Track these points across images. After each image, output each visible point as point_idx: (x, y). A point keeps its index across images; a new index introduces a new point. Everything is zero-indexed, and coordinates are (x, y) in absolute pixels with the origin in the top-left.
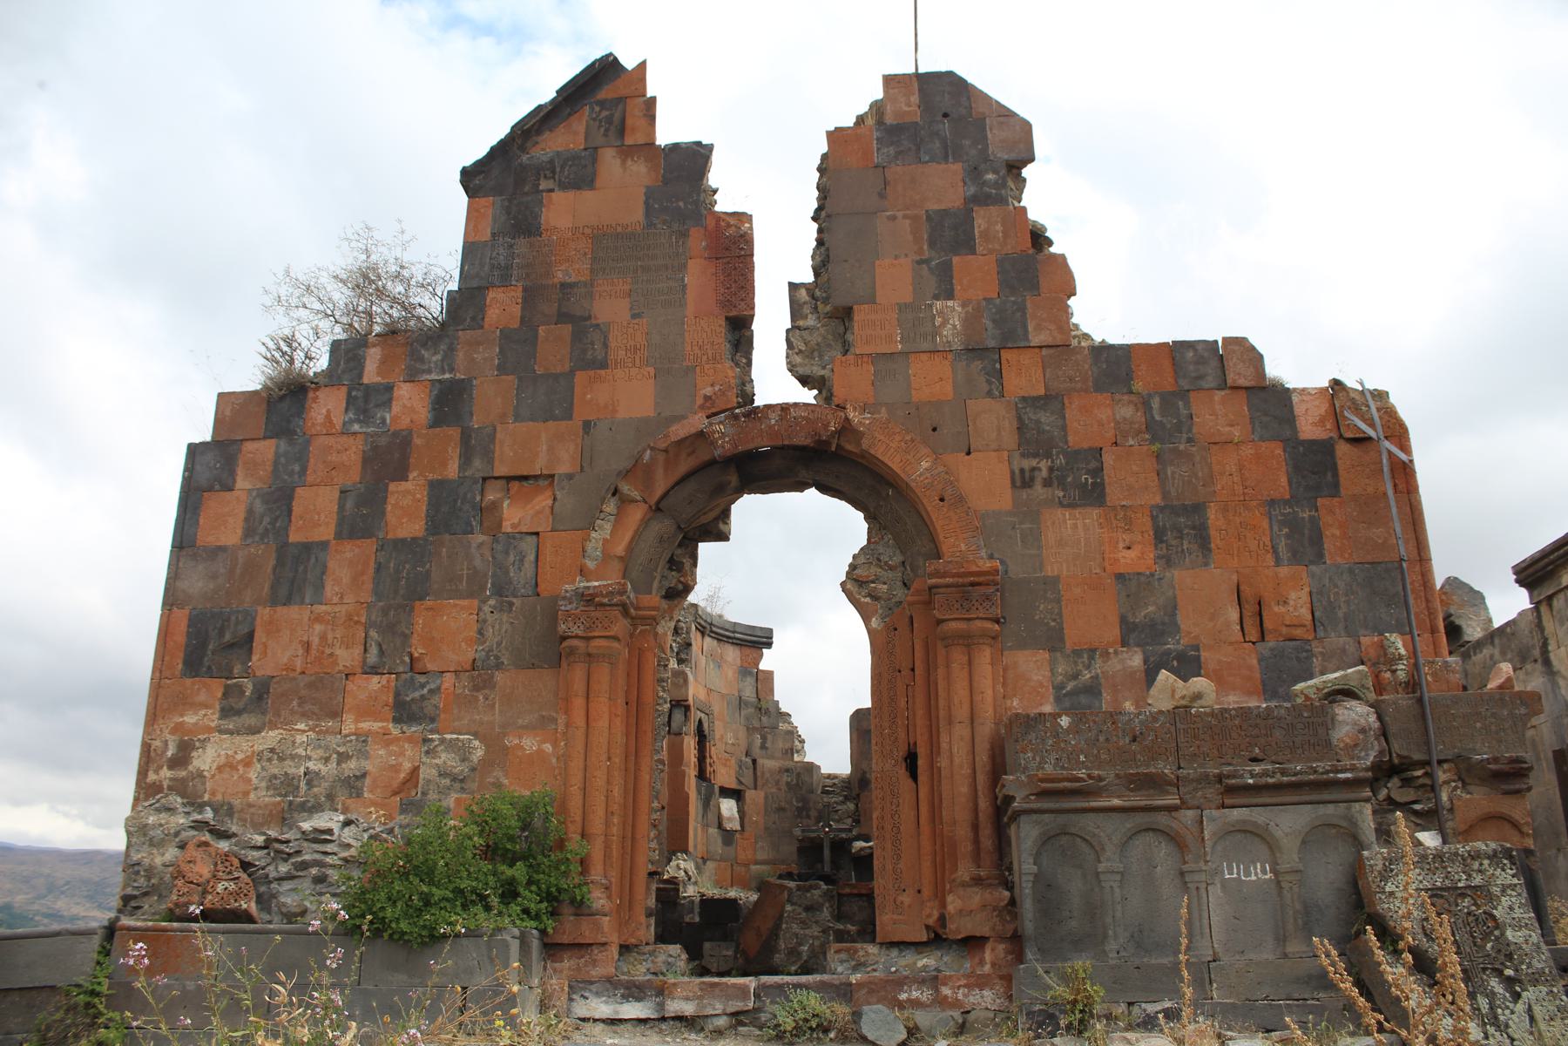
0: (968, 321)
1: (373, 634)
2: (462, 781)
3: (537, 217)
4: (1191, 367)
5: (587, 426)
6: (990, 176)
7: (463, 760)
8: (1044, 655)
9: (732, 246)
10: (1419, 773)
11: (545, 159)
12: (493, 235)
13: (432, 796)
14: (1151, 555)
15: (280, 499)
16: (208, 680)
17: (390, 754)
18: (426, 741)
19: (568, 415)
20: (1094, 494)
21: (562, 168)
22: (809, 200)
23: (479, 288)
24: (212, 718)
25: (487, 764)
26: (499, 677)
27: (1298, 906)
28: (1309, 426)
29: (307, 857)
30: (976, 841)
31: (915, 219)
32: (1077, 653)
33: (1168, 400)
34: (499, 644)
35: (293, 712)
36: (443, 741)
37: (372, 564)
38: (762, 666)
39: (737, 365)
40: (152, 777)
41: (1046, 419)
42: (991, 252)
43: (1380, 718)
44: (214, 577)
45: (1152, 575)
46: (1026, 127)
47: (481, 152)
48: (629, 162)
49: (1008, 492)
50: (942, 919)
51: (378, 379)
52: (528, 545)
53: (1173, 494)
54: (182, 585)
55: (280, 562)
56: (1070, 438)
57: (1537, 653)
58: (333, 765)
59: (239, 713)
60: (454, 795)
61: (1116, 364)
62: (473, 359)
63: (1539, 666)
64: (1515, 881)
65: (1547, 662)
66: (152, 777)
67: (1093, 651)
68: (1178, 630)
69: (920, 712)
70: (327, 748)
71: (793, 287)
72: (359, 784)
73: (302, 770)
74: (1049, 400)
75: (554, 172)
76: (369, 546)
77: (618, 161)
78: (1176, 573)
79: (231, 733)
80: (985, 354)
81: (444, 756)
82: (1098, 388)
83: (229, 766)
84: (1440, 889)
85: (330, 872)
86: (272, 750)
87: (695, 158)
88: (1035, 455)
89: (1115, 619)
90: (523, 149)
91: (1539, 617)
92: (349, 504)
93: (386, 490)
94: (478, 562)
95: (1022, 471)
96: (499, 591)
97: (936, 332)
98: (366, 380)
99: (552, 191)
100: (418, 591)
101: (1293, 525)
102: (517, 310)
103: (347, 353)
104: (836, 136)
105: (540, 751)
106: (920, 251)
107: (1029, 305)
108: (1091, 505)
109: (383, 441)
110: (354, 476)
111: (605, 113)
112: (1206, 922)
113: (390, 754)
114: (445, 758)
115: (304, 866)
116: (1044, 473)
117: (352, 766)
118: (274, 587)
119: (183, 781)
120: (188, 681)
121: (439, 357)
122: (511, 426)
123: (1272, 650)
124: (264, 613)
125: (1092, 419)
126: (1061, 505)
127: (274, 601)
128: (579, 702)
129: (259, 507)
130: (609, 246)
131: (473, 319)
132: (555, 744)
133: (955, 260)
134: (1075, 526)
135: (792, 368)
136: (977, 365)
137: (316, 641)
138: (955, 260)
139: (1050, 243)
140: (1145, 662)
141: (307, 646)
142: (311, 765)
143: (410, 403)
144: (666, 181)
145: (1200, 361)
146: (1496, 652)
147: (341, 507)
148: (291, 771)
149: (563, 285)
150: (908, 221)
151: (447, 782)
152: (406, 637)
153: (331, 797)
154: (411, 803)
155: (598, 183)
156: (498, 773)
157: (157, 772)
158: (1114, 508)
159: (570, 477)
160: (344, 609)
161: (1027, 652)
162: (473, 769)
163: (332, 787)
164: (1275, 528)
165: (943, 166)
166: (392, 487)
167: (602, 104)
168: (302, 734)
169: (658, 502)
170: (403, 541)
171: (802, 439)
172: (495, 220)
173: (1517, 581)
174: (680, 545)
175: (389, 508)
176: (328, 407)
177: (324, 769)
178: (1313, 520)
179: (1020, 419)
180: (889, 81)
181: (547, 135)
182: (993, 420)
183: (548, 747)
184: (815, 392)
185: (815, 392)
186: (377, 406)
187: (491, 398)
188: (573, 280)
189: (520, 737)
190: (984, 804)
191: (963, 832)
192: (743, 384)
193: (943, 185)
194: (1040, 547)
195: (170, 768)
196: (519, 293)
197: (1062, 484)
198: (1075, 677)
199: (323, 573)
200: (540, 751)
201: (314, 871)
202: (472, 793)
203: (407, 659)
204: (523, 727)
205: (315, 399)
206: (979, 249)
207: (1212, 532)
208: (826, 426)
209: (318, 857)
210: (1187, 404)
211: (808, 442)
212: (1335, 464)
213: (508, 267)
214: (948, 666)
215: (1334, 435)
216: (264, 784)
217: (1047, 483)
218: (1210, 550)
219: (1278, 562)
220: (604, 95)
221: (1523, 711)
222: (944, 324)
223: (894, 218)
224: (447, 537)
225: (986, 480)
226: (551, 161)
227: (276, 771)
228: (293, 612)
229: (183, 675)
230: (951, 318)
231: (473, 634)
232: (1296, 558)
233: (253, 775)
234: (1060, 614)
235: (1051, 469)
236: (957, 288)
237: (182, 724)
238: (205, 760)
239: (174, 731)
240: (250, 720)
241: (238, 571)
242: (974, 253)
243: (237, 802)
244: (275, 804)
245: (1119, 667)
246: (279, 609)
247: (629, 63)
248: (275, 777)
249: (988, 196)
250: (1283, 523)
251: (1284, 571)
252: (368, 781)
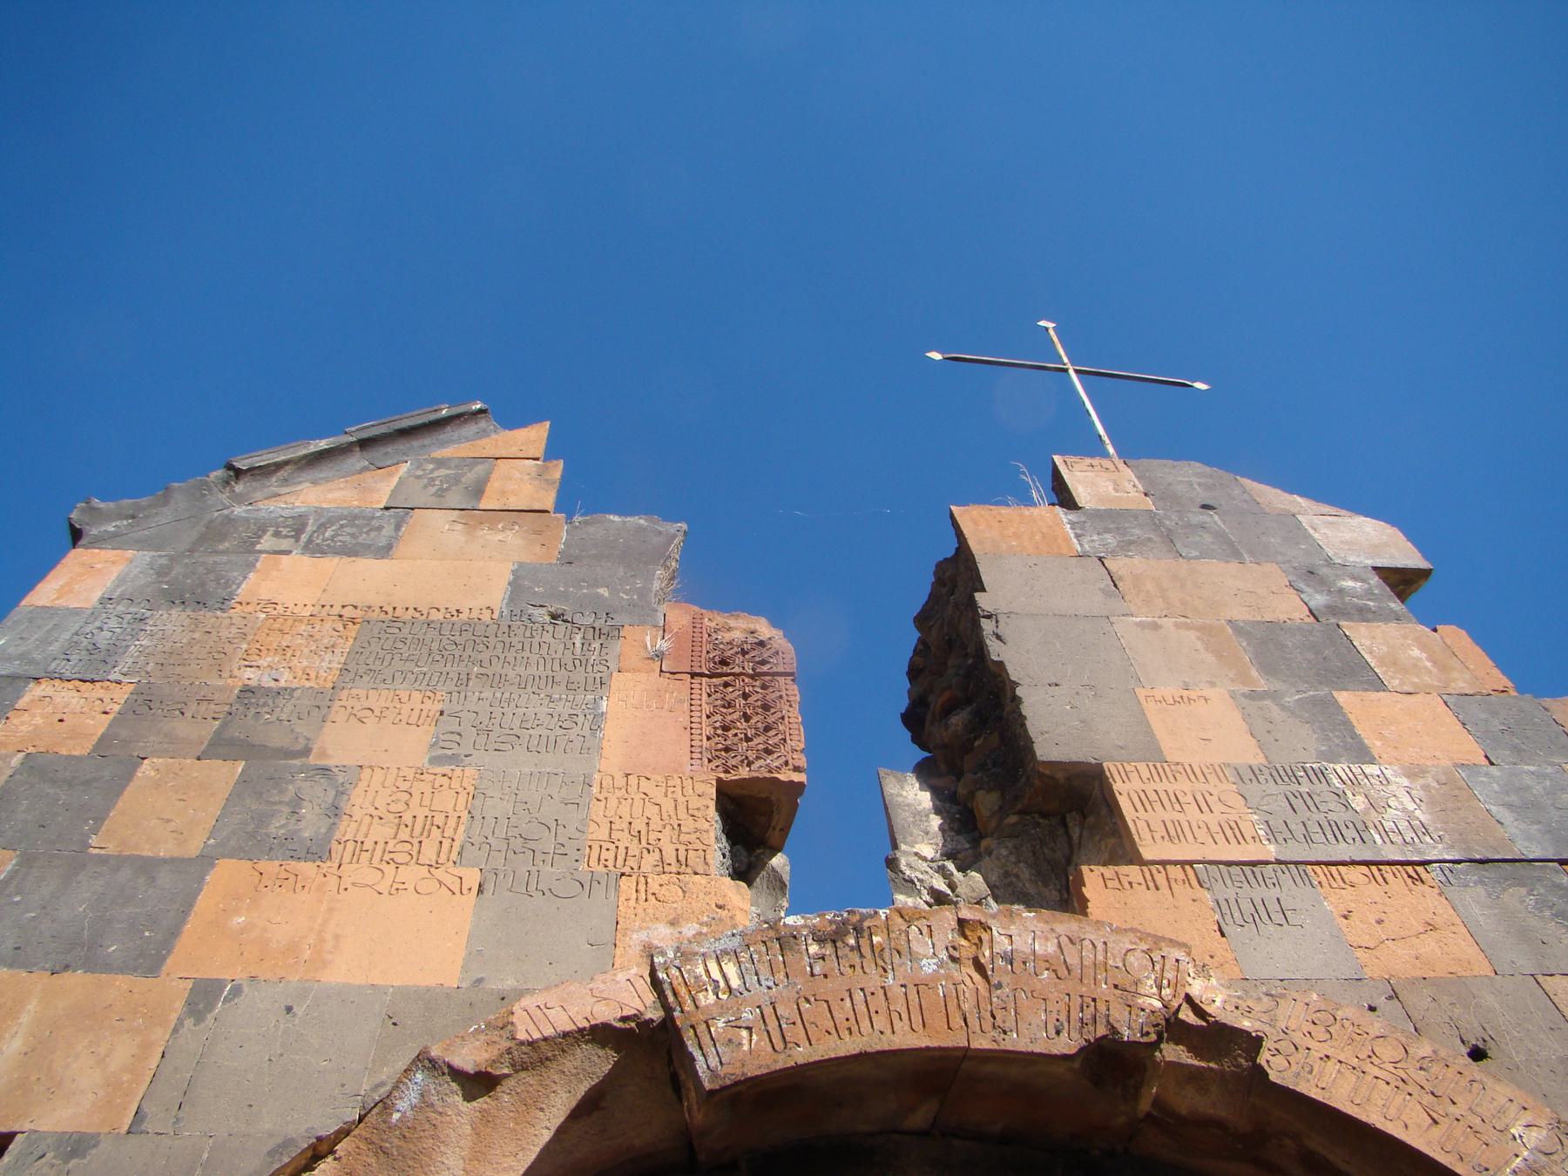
5: (204, 996)
6: (1349, 584)
11: (286, 513)
12: (107, 600)
21: (323, 527)
23: (13, 678)
31: (1204, 630)
99: (288, 552)
102: (98, 725)
111: (443, 472)
133: (1342, 697)
149: (247, 690)
150: (1192, 635)
167: (441, 463)
172: (121, 580)
188: (282, 683)
206: (1394, 683)
208: (1127, 991)
211: (1067, 1044)
236: (1375, 745)
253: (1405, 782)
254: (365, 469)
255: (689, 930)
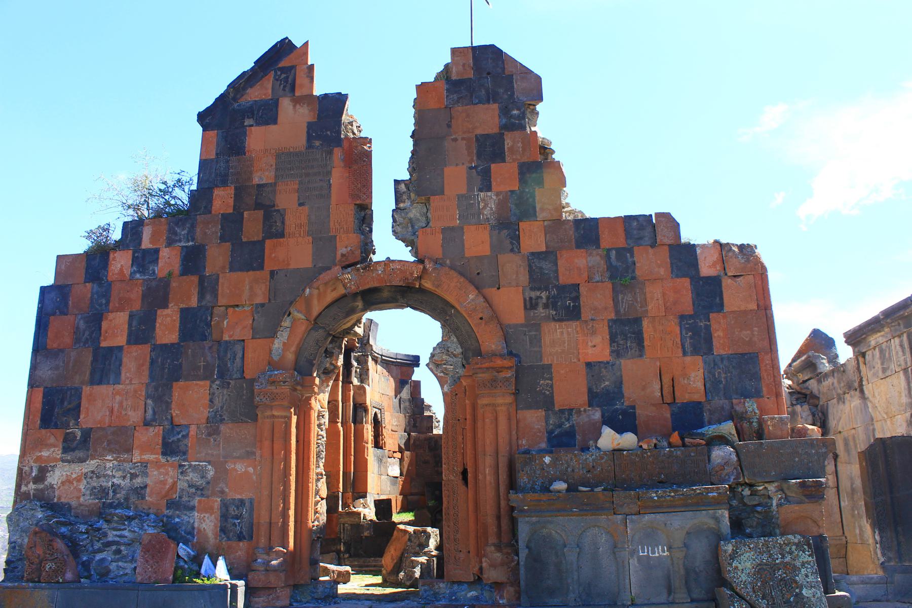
0: (501, 205)
1: (149, 402)
2: (202, 490)
3: (243, 142)
4: (635, 232)
5: (272, 273)
7: (202, 477)
8: (541, 413)
9: (359, 158)
10: (761, 488)
12: (217, 154)
13: (185, 499)
14: (607, 352)
15: (96, 320)
16: (54, 431)
17: (160, 474)
18: (181, 466)
19: (261, 267)
20: (573, 313)
22: (409, 126)
24: (58, 453)
25: (216, 479)
26: (222, 427)
27: (682, 572)
28: (706, 269)
29: (110, 539)
30: (499, 526)
32: (562, 411)
33: (621, 252)
34: (222, 408)
35: (104, 449)
36: (190, 466)
37: (148, 358)
38: (414, 378)
39: (363, 233)
40: (24, 488)
41: (546, 266)
42: (514, 160)
43: (738, 455)
44: (57, 368)
45: (608, 363)
46: (538, 79)
47: (210, 102)
48: (298, 106)
49: (523, 311)
50: (481, 569)
51: (151, 246)
52: (238, 348)
53: (622, 311)
54: (39, 373)
55: (95, 359)
56: (561, 278)
57: (856, 385)
58: (128, 480)
59: (73, 450)
60: (197, 498)
61: (588, 231)
62: (205, 233)
63: (857, 393)
64: (810, 559)
65: (862, 391)
66: (24, 488)
67: (571, 410)
68: (623, 397)
69: (469, 445)
70: (124, 470)
71: (397, 182)
72: (143, 492)
73: (110, 484)
74: (549, 255)
75: (253, 114)
76: (147, 348)
77: (291, 107)
78: (622, 361)
79: (69, 462)
80: (508, 227)
81: (191, 475)
82: (578, 246)
83: (68, 481)
84: (766, 565)
85: (123, 548)
86: (93, 472)
87: (337, 102)
88: (539, 289)
89: (585, 390)
90: (235, 99)
91: (858, 363)
92: (134, 323)
93: (156, 314)
94: (209, 358)
95: (531, 298)
96: (221, 375)
97: (480, 212)
98: (143, 247)
99: (252, 126)
100: (175, 375)
101: (695, 331)
102: (231, 202)
103: (132, 229)
104: (422, 88)
105: (246, 472)
106: (471, 161)
107: (537, 193)
108: (571, 320)
109: (154, 284)
110: (137, 306)
111: (283, 76)
112: (627, 581)
113: (160, 474)
114: (192, 476)
115: (109, 544)
116: (544, 301)
117: (138, 481)
118: (92, 374)
119: (42, 490)
120: (43, 431)
121: (185, 232)
122: (228, 275)
123: (679, 408)
124: (86, 390)
125: (576, 265)
126: (554, 320)
127: (92, 382)
128: (267, 443)
129: (82, 325)
130: (286, 161)
131: (205, 207)
132: (255, 468)
133: (493, 166)
134: (562, 333)
135: (395, 232)
136: (505, 232)
137: (116, 406)
138: (493, 166)
139: (553, 152)
140: (603, 416)
141: (112, 411)
142: (115, 480)
143: (169, 260)
144: (319, 117)
145: (641, 228)
146: (835, 381)
147: (130, 325)
148: (104, 484)
149: (259, 186)
151: (193, 490)
152: (168, 405)
153: (127, 499)
154: (173, 503)
155: (281, 118)
156: (222, 485)
157: (26, 486)
158: (586, 322)
159: (263, 305)
160: (132, 387)
161: (533, 411)
162: (208, 483)
163: (128, 494)
164: (684, 332)
165: (486, 106)
166: (159, 312)
167: (283, 70)
168: (110, 462)
169: (315, 320)
170: (165, 345)
171: (397, 282)
173: (846, 342)
174: (331, 342)
175: (158, 325)
176: (121, 262)
177: (123, 483)
178: (706, 326)
179: (530, 266)
180: (455, 51)
181: (249, 91)
182: (514, 269)
183: (251, 470)
184: (410, 248)
185: (410, 248)
186: (150, 262)
187: (217, 257)
189: (235, 464)
190: (503, 503)
191: (491, 520)
192: (366, 244)
193: (486, 118)
194: (540, 346)
195: (34, 483)
196: (233, 192)
197: (555, 307)
198: (560, 426)
199: (120, 365)
200: (246, 472)
201: (114, 548)
202: (208, 497)
203: (169, 417)
204: (238, 458)
205: (114, 259)
206: (508, 159)
207: (645, 336)
208: (412, 274)
209: (117, 539)
210: (632, 256)
212: (721, 292)
213: (226, 175)
214: (484, 421)
215: (722, 273)
216: (88, 492)
217: (546, 306)
218: (643, 347)
219: (685, 354)
220: (282, 63)
221: (824, 450)
222: (484, 208)
223: (455, 140)
224: (191, 343)
225: (511, 302)
226: (251, 107)
227: (95, 484)
228: (103, 389)
229: (41, 427)
230: (489, 203)
231: (207, 402)
232: (696, 351)
233: (82, 487)
234: (552, 386)
235: (548, 298)
236: (494, 184)
237: (41, 457)
238: (55, 478)
239: (35, 462)
240: (80, 454)
241: (71, 365)
242: (504, 161)
243: (74, 503)
244: (95, 504)
245: (586, 420)
246: (95, 387)
247: (298, 43)
248: (95, 488)
249: (513, 125)
250: (688, 330)
251: (688, 359)
252: (148, 490)
253: (494, 197)
254: (263, 77)
255: (349, 249)
